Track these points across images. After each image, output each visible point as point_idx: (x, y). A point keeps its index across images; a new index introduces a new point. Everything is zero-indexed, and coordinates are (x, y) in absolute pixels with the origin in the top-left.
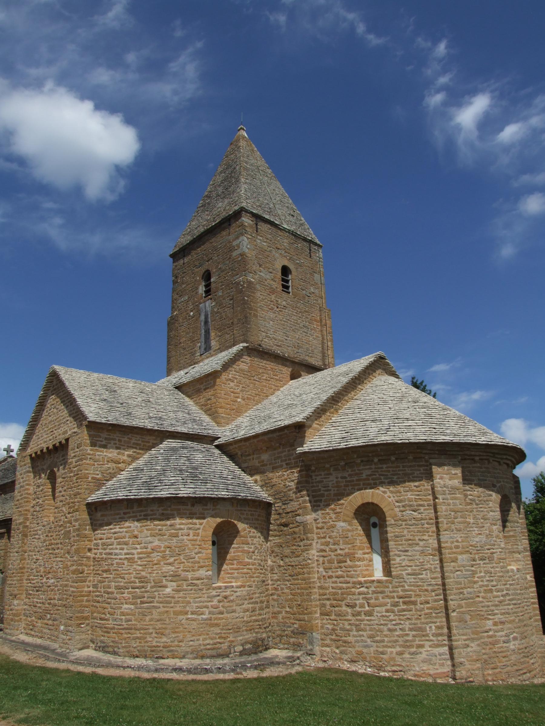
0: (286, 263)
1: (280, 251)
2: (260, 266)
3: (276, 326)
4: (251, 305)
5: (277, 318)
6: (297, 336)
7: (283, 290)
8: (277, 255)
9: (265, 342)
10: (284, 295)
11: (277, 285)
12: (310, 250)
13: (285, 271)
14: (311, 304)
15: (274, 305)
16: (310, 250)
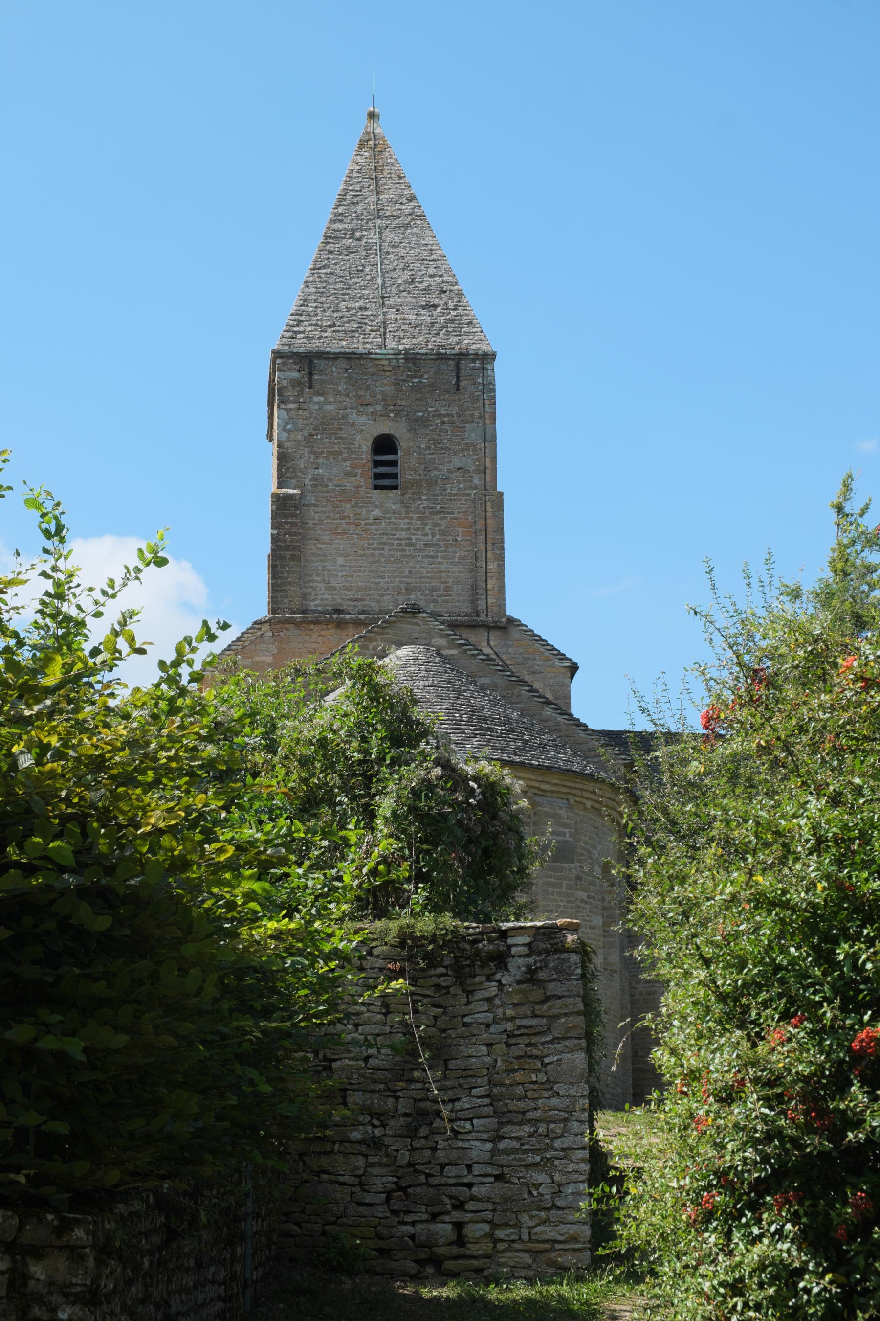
0: (385, 428)
1: (371, 409)
2: (317, 455)
3: (354, 563)
4: (285, 541)
5: (355, 549)
6: (407, 570)
7: (376, 487)
8: (364, 419)
9: (322, 600)
10: (377, 496)
11: (363, 481)
12: (458, 377)
13: (384, 445)
14: (451, 495)
15: (347, 524)
16: (458, 377)
